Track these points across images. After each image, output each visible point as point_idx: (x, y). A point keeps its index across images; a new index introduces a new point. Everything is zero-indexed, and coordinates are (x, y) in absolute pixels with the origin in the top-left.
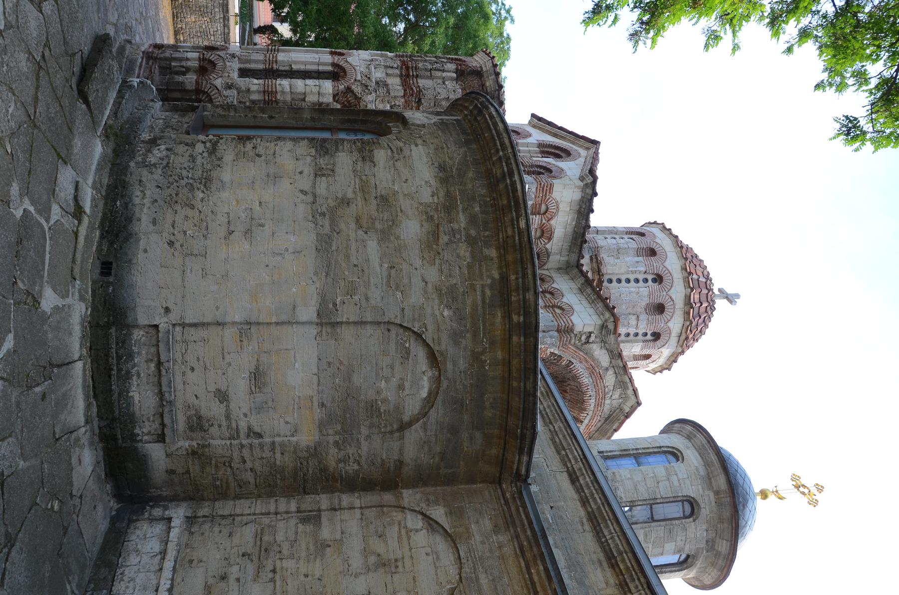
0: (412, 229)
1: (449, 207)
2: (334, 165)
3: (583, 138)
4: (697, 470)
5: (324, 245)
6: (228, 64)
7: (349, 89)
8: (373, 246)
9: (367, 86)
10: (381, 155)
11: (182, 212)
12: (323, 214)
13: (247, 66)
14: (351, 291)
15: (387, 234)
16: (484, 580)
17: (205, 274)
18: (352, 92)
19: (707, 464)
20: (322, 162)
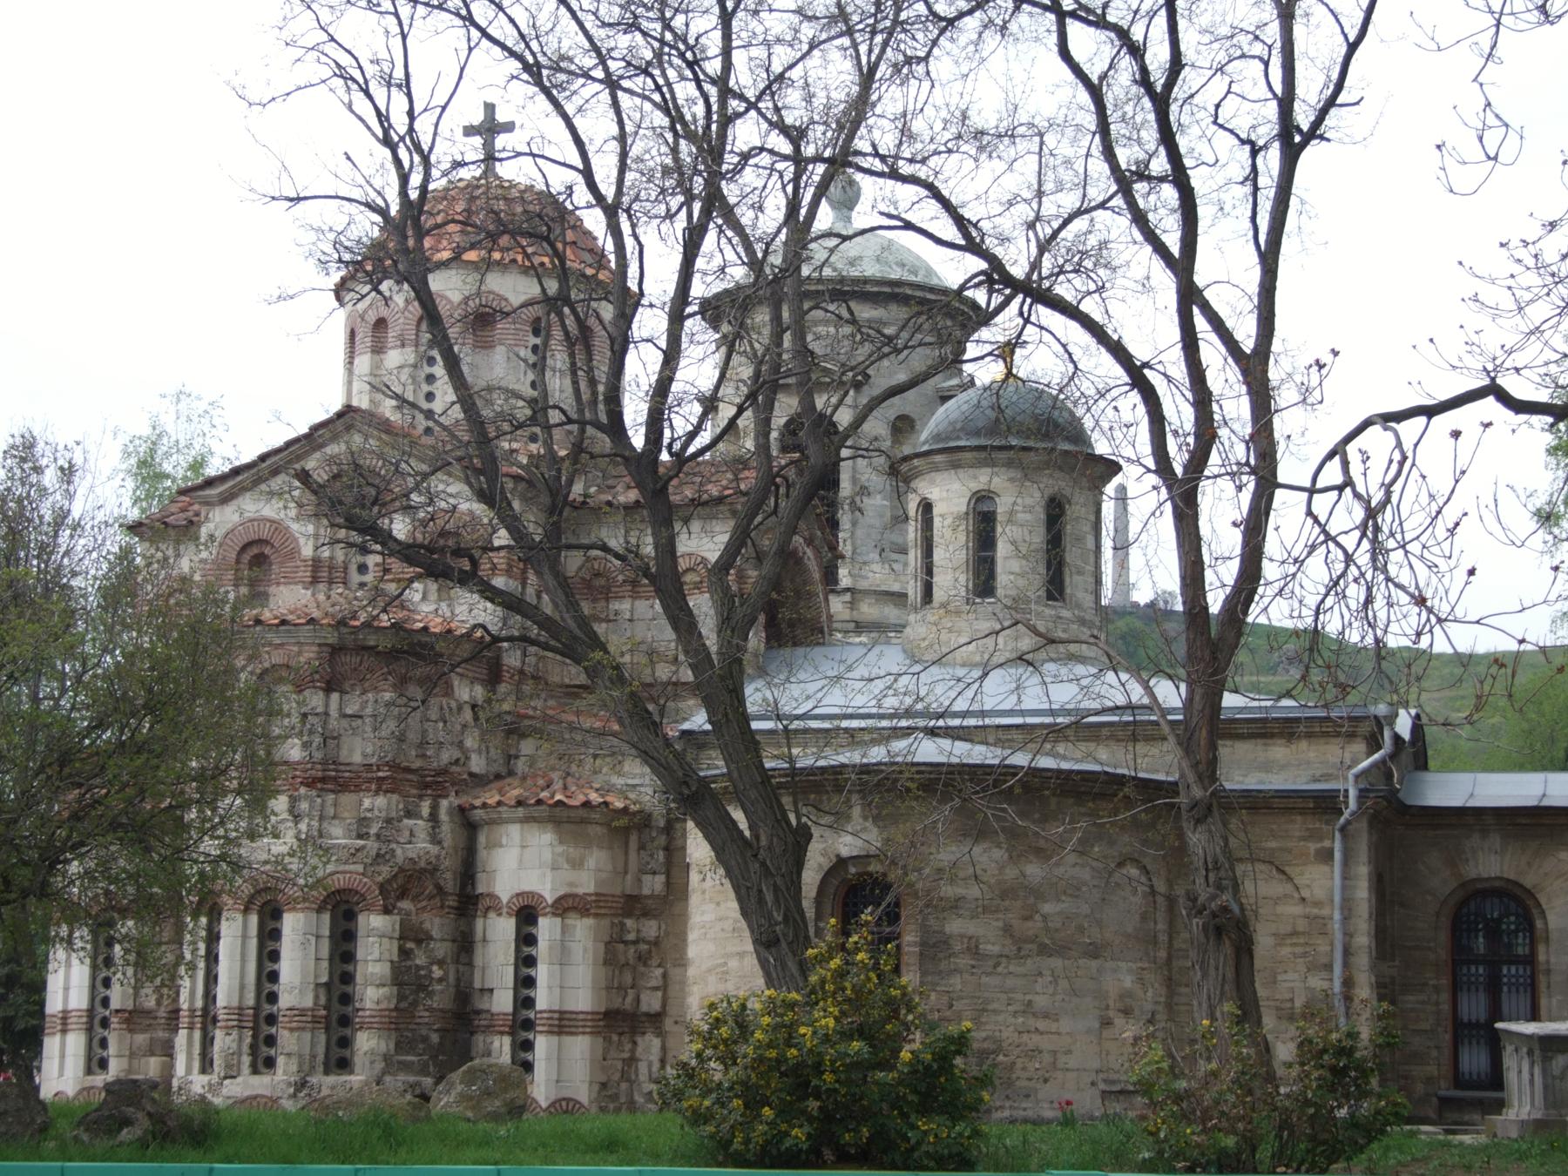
0: (1034, 871)
1: (1013, 834)
2: (962, 936)
3: (315, 429)
4: (1011, 480)
5: (1044, 950)
7: (382, 888)
8: (1047, 908)
9: (378, 855)
10: (948, 891)
11: (1018, 1073)
12: (1019, 949)
13: (321, 1058)
14: (1081, 929)
15: (1038, 894)
16: (1273, 844)
17: (1069, 1052)
18: (389, 881)
19: (1009, 464)
20: (958, 947)
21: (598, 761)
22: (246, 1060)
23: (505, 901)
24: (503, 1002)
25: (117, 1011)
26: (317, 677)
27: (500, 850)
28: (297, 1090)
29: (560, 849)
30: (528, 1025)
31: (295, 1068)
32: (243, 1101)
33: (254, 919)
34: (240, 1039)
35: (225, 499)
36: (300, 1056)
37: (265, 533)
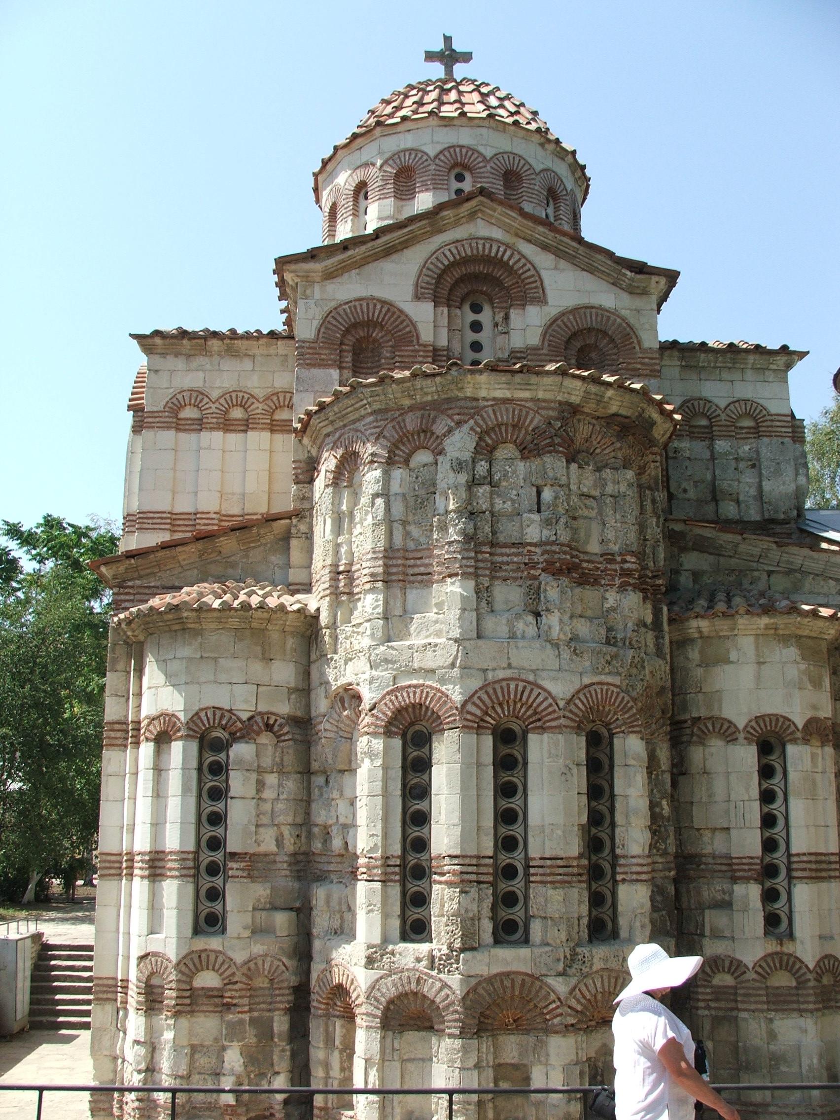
6: (598, 965)
13: (585, 921)
21: (773, 578)
22: (487, 926)
23: (741, 726)
24: (748, 843)
25: (233, 855)
26: (557, 440)
27: (727, 667)
28: (568, 966)
29: (803, 667)
30: (770, 871)
31: (563, 936)
32: (490, 980)
33: (488, 741)
34: (480, 900)
35: (330, 275)
36: (568, 919)
37: (377, 313)
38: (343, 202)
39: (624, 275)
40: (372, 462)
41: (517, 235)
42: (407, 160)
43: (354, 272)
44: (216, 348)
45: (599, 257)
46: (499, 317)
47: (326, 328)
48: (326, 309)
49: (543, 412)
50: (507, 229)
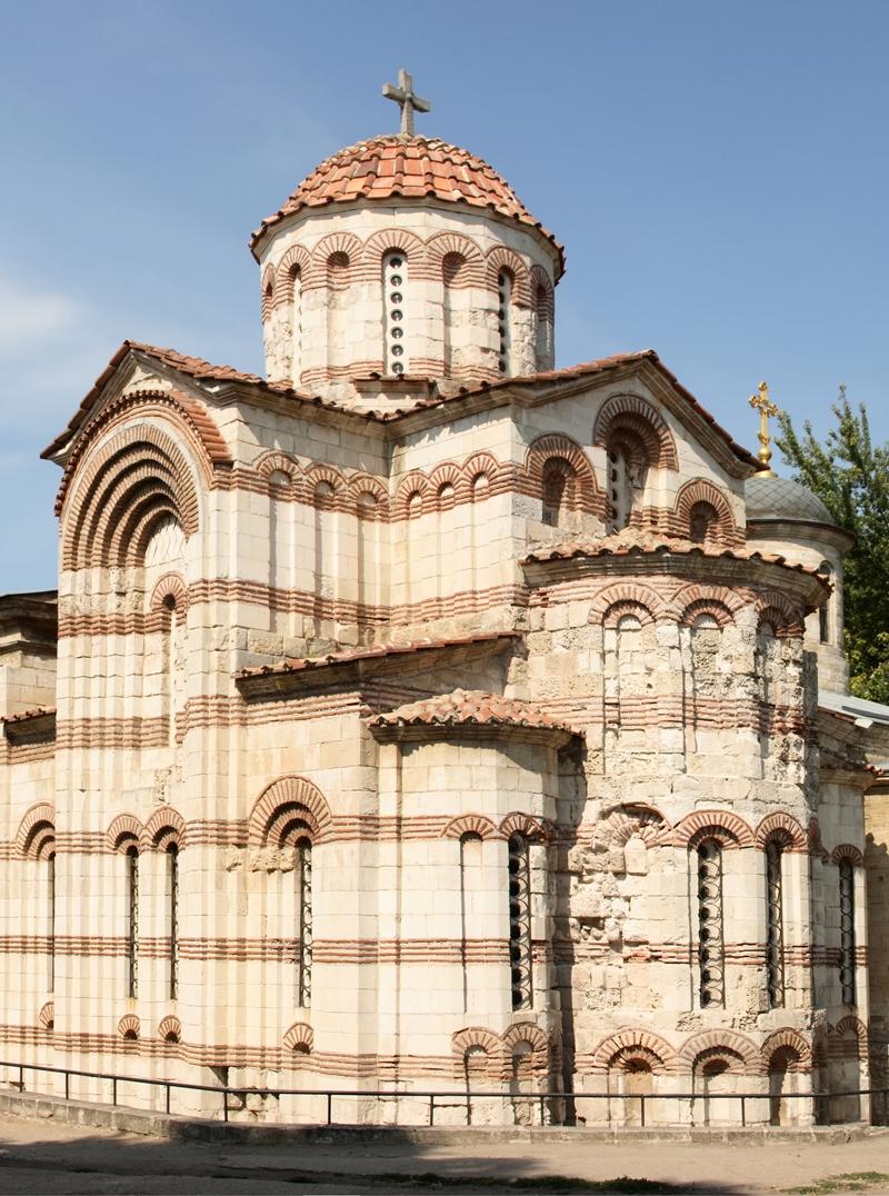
38: (363, 260)
39: (733, 460)
40: (667, 617)
41: (662, 401)
42: (456, 245)
43: (551, 405)
44: (308, 414)
45: (720, 439)
46: (634, 472)
47: (533, 458)
48: (532, 437)
49: (795, 603)
50: (656, 392)
